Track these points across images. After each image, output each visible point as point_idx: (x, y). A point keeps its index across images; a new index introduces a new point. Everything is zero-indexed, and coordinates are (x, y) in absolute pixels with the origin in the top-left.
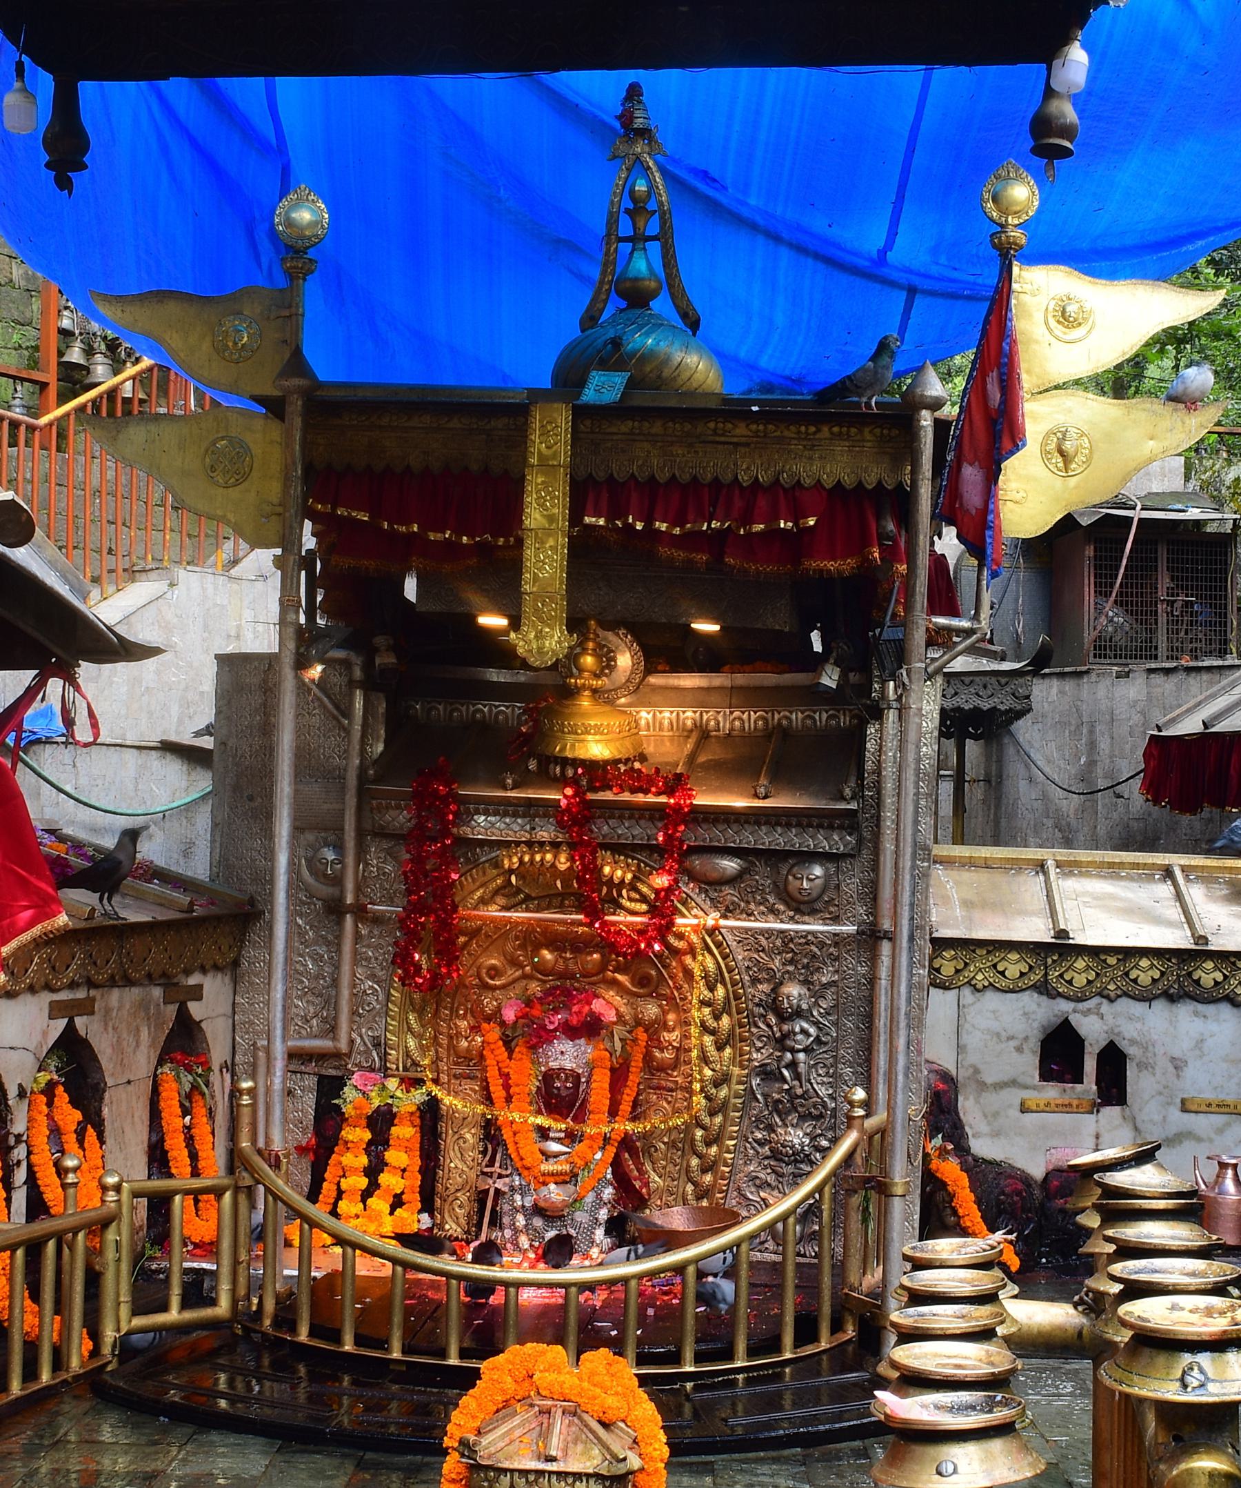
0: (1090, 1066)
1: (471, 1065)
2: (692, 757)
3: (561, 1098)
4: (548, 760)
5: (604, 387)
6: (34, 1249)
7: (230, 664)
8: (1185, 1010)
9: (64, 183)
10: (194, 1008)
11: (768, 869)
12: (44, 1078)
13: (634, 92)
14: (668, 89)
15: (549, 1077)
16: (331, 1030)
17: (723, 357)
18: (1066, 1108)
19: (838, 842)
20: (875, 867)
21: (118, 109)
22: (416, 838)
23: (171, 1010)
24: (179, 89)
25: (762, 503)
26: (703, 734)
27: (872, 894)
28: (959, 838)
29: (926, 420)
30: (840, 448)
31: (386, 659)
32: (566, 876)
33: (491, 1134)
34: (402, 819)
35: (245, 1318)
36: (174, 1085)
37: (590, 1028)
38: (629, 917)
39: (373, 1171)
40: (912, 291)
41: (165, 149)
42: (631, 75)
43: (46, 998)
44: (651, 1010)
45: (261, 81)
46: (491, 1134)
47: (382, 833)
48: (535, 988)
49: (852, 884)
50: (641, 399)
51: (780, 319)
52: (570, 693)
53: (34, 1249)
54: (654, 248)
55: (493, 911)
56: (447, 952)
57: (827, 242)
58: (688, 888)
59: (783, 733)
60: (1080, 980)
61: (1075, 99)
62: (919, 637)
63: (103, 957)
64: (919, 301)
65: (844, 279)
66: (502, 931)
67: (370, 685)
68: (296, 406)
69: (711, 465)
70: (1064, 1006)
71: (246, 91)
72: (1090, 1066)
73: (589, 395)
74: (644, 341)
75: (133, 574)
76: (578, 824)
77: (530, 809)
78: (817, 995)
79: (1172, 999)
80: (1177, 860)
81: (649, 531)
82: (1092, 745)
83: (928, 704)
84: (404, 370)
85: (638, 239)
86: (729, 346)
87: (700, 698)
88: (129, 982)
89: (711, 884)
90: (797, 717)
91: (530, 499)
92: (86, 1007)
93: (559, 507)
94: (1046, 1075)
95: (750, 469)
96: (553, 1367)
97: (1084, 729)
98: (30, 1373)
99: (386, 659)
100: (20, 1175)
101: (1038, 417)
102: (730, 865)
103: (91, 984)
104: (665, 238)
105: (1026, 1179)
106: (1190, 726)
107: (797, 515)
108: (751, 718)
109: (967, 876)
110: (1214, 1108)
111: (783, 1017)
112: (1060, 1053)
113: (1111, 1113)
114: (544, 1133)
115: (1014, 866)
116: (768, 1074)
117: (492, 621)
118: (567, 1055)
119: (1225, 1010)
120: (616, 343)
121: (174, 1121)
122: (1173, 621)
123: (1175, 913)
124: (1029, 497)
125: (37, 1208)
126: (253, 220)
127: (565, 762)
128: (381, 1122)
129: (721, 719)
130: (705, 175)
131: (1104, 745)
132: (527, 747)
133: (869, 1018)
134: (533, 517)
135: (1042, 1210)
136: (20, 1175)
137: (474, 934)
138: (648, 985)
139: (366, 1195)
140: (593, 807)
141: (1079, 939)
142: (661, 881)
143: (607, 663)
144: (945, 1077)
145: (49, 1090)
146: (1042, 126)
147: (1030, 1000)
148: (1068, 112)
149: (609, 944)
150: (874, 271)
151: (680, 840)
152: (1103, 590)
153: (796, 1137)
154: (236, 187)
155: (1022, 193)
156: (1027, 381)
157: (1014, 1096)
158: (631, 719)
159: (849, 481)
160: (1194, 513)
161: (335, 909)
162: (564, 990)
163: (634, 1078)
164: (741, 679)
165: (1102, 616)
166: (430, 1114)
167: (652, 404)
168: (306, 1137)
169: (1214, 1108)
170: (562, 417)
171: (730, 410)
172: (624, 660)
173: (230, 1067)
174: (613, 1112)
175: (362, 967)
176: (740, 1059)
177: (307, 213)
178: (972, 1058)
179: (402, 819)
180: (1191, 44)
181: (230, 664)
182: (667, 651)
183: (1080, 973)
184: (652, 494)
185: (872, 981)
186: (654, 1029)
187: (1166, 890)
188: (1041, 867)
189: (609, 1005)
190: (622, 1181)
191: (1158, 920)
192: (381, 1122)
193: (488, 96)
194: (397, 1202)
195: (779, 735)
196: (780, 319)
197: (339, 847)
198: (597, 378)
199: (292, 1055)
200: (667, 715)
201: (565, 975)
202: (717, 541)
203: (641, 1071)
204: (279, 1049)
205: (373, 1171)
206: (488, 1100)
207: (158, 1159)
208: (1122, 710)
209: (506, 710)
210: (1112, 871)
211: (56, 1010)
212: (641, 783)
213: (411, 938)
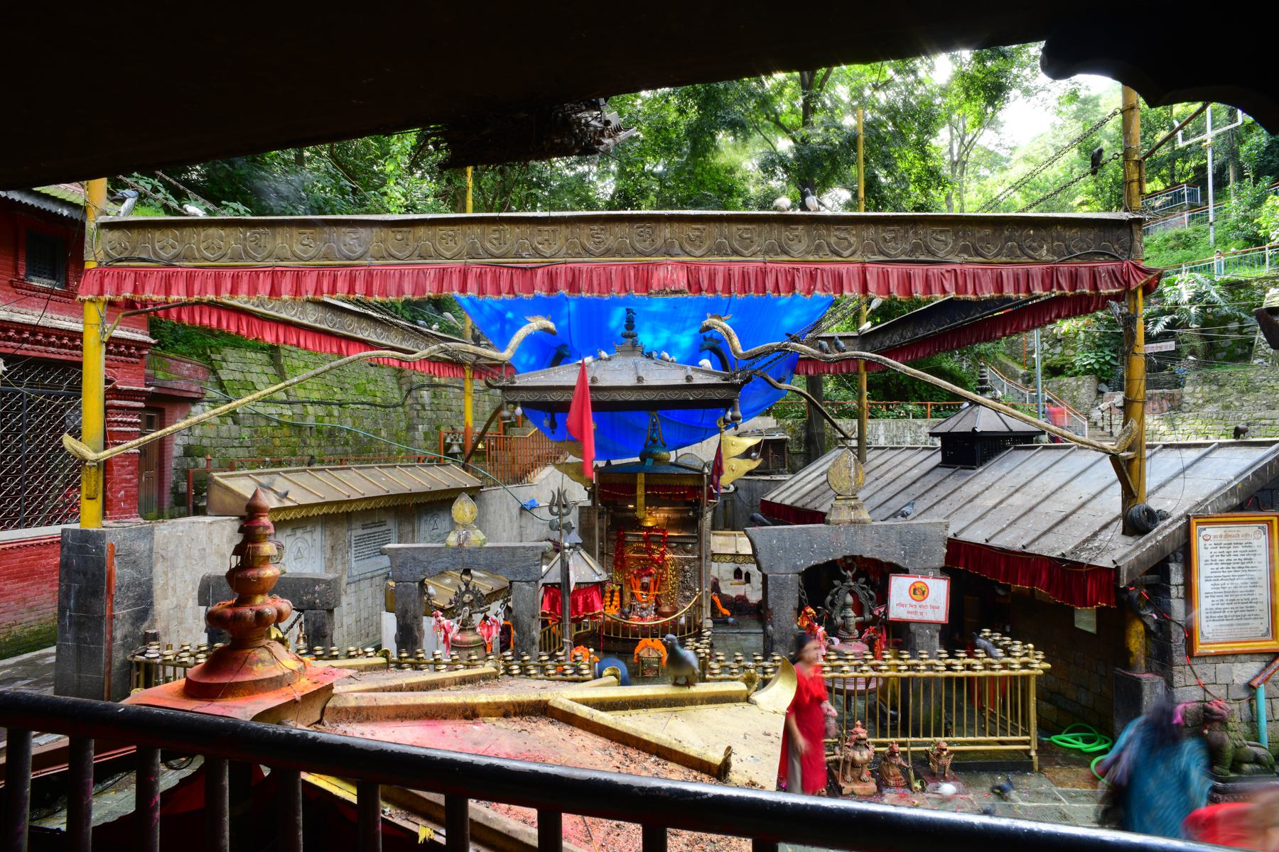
11: (681, 546)
27: (700, 550)
35: (593, 631)
37: (650, 575)
46: (633, 595)
56: (623, 562)
76: (647, 539)
87: (668, 512)
89: (671, 548)
95: (676, 482)
108: (677, 516)
112: (738, 574)
118: (646, 580)
128: (612, 592)
138: (660, 566)
149: (653, 560)
151: (665, 541)
153: (688, 594)
158: (654, 518)
160: (777, 436)
166: (621, 591)
183: (741, 559)
184: (659, 487)
189: (653, 570)
192: (612, 592)
195: (682, 519)
203: (660, 582)
212: (657, 531)
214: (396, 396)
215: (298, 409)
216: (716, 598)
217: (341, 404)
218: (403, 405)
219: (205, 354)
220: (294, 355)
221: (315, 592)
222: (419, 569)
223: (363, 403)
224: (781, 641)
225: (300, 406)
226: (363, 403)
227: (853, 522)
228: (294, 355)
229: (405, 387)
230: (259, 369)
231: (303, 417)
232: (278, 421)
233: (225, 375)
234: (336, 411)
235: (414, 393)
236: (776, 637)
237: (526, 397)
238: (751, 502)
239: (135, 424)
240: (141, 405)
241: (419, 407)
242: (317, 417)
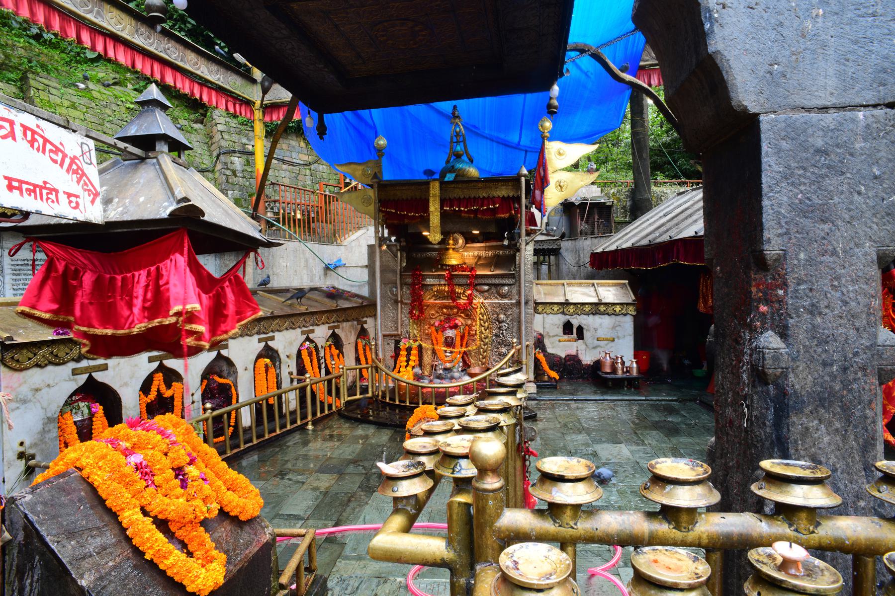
0: (575, 331)
1: (429, 336)
2: (476, 263)
3: (449, 343)
4: (442, 265)
5: (450, 177)
6: (330, 382)
7: (369, 246)
8: (597, 317)
9: (321, 138)
10: (365, 326)
11: (495, 288)
12: (328, 343)
13: (455, 107)
14: (462, 104)
15: (446, 338)
16: (397, 329)
17: (479, 169)
18: (569, 341)
19: (511, 281)
20: (520, 286)
21: (334, 120)
22: (413, 285)
23: (359, 327)
24: (348, 114)
25: (486, 202)
26: (479, 258)
28: (550, 279)
29: (523, 179)
30: (503, 188)
31: (404, 244)
32: (447, 292)
33: (434, 352)
34: (409, 280)
36: (361, 343)
37: (455, 327)
38: (463, 301)
39: (408, 361)
40: (526, 151)
41: (347, 129)
42: (454, 102)
43: (327, 325)
44: (469, 322)
45: (367, 111)
46: (434, 352)
47: (406, 284)
48: (442, 318)
49: (514, 291)
50: (459, 179)
51: (495, 160)
52: (448, 249)
53: (330, 382)
54: (462, 144)
55: (432, 301)
56: (421, 311)
57: (505, 140)
58: (475, 293)
59: (498, 256)
60: (572, 311)
61: (557, 99)
62: (523, 232)
63: (342, 315)
64: (528, 154)
65: (509, 149)
66: (433, 306)
67: (402, 249)
68: (376, 186)
69: (473, 194)
70: (568, 317)
71: (365, 113)
72: (575, 331)
73: (446, 179)
74: (460, 166)
75: (359, 228)
76: (450, 279)
77: (439, 277)
78: (507, 317)
79: (594, 314)
80: (595, 282)
81: (460, 211)
82: (579, 256)
83: (530, 248)
84: (407, 176)
85: (458, 142)
86: (483, 167)
87: (479, 249)
88: (348, 321)
89: (482, 292)
90: (501, 252)
91: (431, 204)
92: (338, 327)
93: (438, 206)
94: (564, 333)
95: (482, 194)
96: (431, 410)
97: (577, 252)
98: (322, 411)
99: (404, 244)
100: (323, 366)
101: (553, 178)
102: (486, 288)
103: (338, 322)
104: (464, 141)
105: (560, 358)
106: (600, 250)
107: (494, 204)
108: (490, 253)
109: (545, 287)
110: (604, 340)
111: (500, 323)
112: (568, 328)
113: (580, 342)
114: (446, 351)
115: (557, 284)
116: (497, 336)
117: (425, 233)
118: (450, 333)
119: (606, 316)
120: (453, 167)
121: (361, 352)
122: (598, 226)
123: (594, 294)
124: (553, 197)
125: (328, 372)
126: (369, 144)
127: (446, 265)
129: (483, 254)
131: (582, 255)
132: (438, 263)
133: (520, 322)
134: (432, 209)
135: (565, 365)
136: (323, 366)
137: (428, 306)
138: (468, 316)
139: (406, 366)
140: (452, 275)
141: (571, 301)
142: (469, 292)
143: (456, 241)
144: (541, 335)
145: (330, 346)
146: (550, 106)
147: (560, 316)
148: (555, 102)
149: (458, 307)
150: (517, 147)
151: (474, 282)
152: (582, 220)
153: (504, 350)
154: (364, 136)
155: (548, 124)
156: (550, 169)
157: (557, 338)
158: (462, 255)
159: (506, 195)
160: (603, 201)
161: (396, 302)
162: (449, 319)
163: (466, 337)
164: (488, 244)
165: (582, 226)
166: (420, 348)
167: (463, 180)
168: (392, 354)
169: (604, 340)
170: (437, 184)
171: (478, 180)
172: (461, 241)
174: (461, 346)
175: (403, 314)
176: (490, 333)
177: (382, 142)
178: (547, 330)
179: (409, 280)
180: (589, 85)
181: (369, 246)
182: (470, 239)
183: (572, 309)
184: (460, 201)
185: (520, 313)
186: (470, 326)
187: (592, 289)
188: (563, 284)
190: (464, 361)
191: (590, 296)
192: (409, 350)
193: (418, 110)
194: (413, 367)
195: (497, 257)
196: (495, 160)
197: (396, 287)
198: (448, 175)
199: (384, 336)
200: (471, 253)
201: (449, 315)
202: (475, 212)
203: (467, 336)
204: (380, 335)
205: (408, 361)
206: (433, 344)
207: (358, 360)
208: (585, 247)
209: (434, 254)
210: (580, 285)
211: (330, 328)
213: (413, 308)
216: (541, 356)
218: (213, 171)
220: (53, 91)
224: (824, 399)
228: (53, 91)
229: (215, 154)
235: (222, 158)
236: (801, 381)
238: (578, 263)
241: (228, 173)
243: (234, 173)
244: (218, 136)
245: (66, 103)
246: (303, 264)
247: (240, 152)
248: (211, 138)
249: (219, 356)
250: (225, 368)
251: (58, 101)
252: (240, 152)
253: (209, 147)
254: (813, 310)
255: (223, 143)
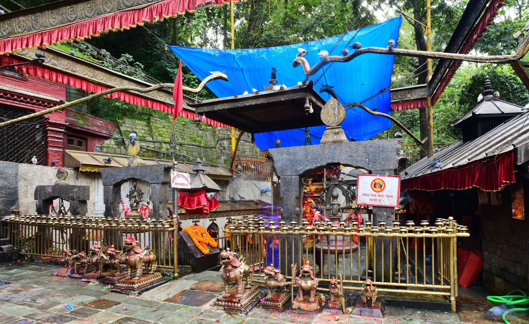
87: (318, 185)
130: (317, 134)
173: (319, 230)
177: (279, 142)
214: (213, 144)
215: (157, 145)
217: (181, 145)
218: (215, 148)
219: (116, 120)
220: (158, 122)
221: (74, 192)
222: (113, 179)
223: (193, 145)
225: (159, 143)
226: (193, 145)
227: (334, 142)
228: (158, 122)
229: (216, 140)
230: (141, 127)
231: (160, 148)
232: (146, 149)
233: (122, 129)
234: (178, 148)
235: (219, 142)
237: (206, 109)
239: (60, 138)
240: (63, 130)
241: (222, 148)
242: (167, 149)
243: (224, 148)
244: (218, 132)
245: (162, 126)
246: (251, 190)
247: (227, 139)
248: (215, 133)
249: (213, 223)
250: (215, 227)
251: (159, 125)
252: (227, 139)
253: (214, 137)
254: (287, 205)
255: (220, 135)
